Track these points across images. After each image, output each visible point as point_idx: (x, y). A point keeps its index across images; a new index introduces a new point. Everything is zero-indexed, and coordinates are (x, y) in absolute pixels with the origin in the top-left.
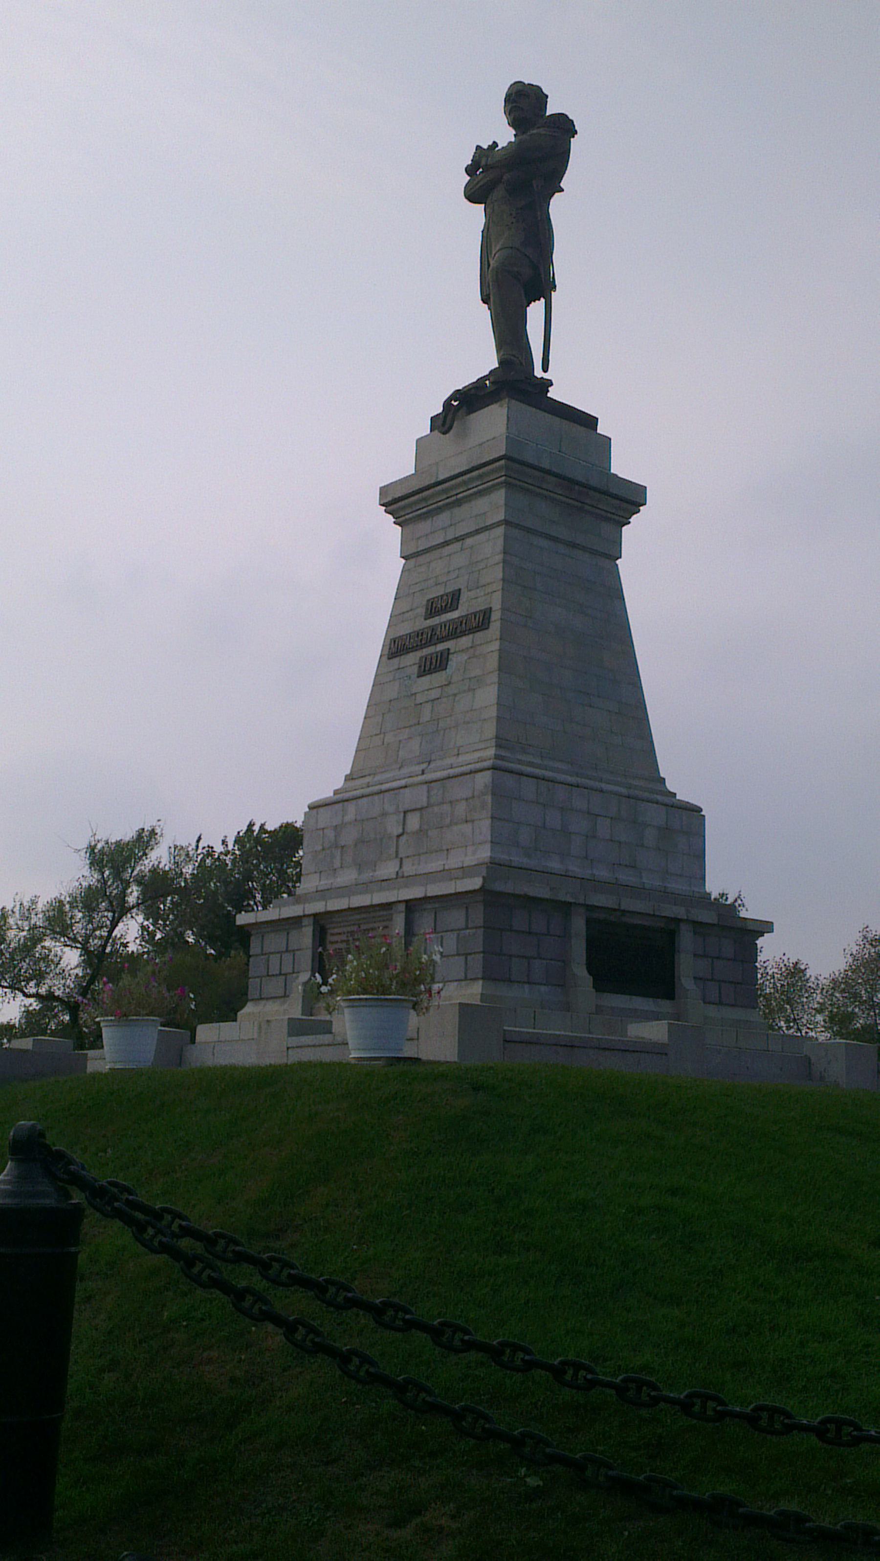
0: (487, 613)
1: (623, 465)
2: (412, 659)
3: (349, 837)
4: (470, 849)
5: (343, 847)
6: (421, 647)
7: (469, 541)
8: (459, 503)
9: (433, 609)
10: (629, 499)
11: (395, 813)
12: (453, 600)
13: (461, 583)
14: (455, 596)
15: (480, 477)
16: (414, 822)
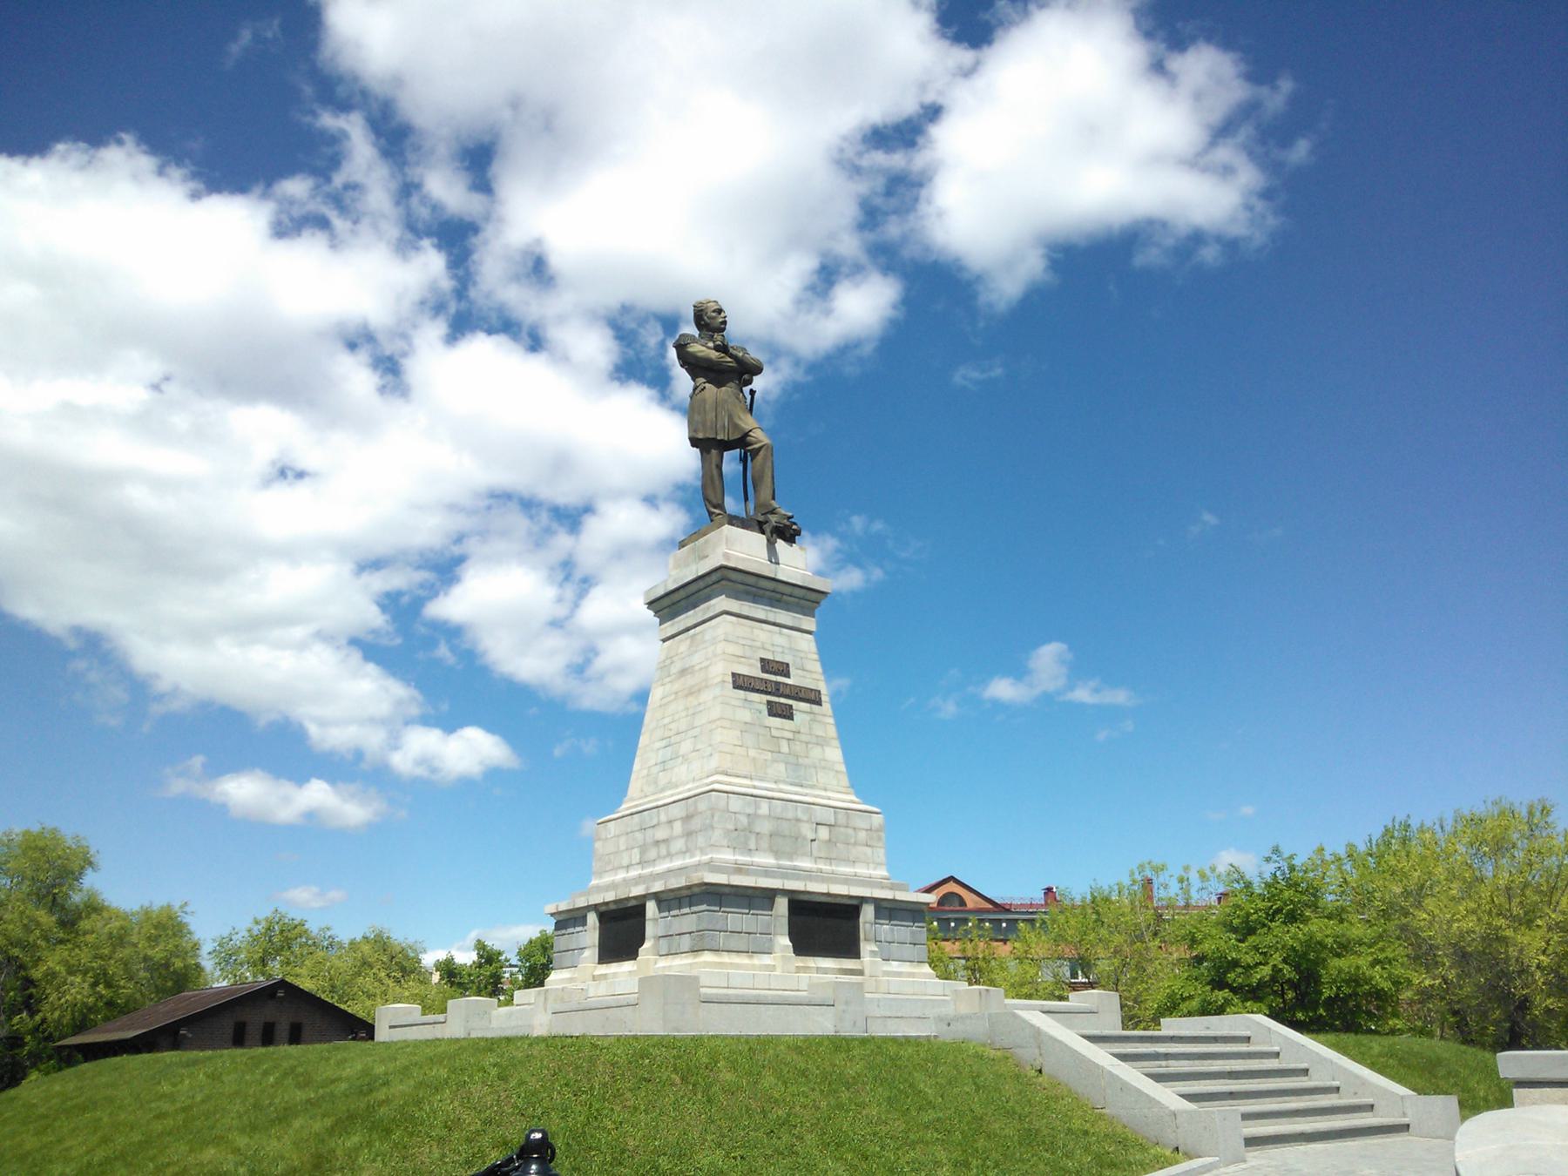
2: (760, 699)
3: (765, 827)
9: (766, 665)
12: (784, 670)
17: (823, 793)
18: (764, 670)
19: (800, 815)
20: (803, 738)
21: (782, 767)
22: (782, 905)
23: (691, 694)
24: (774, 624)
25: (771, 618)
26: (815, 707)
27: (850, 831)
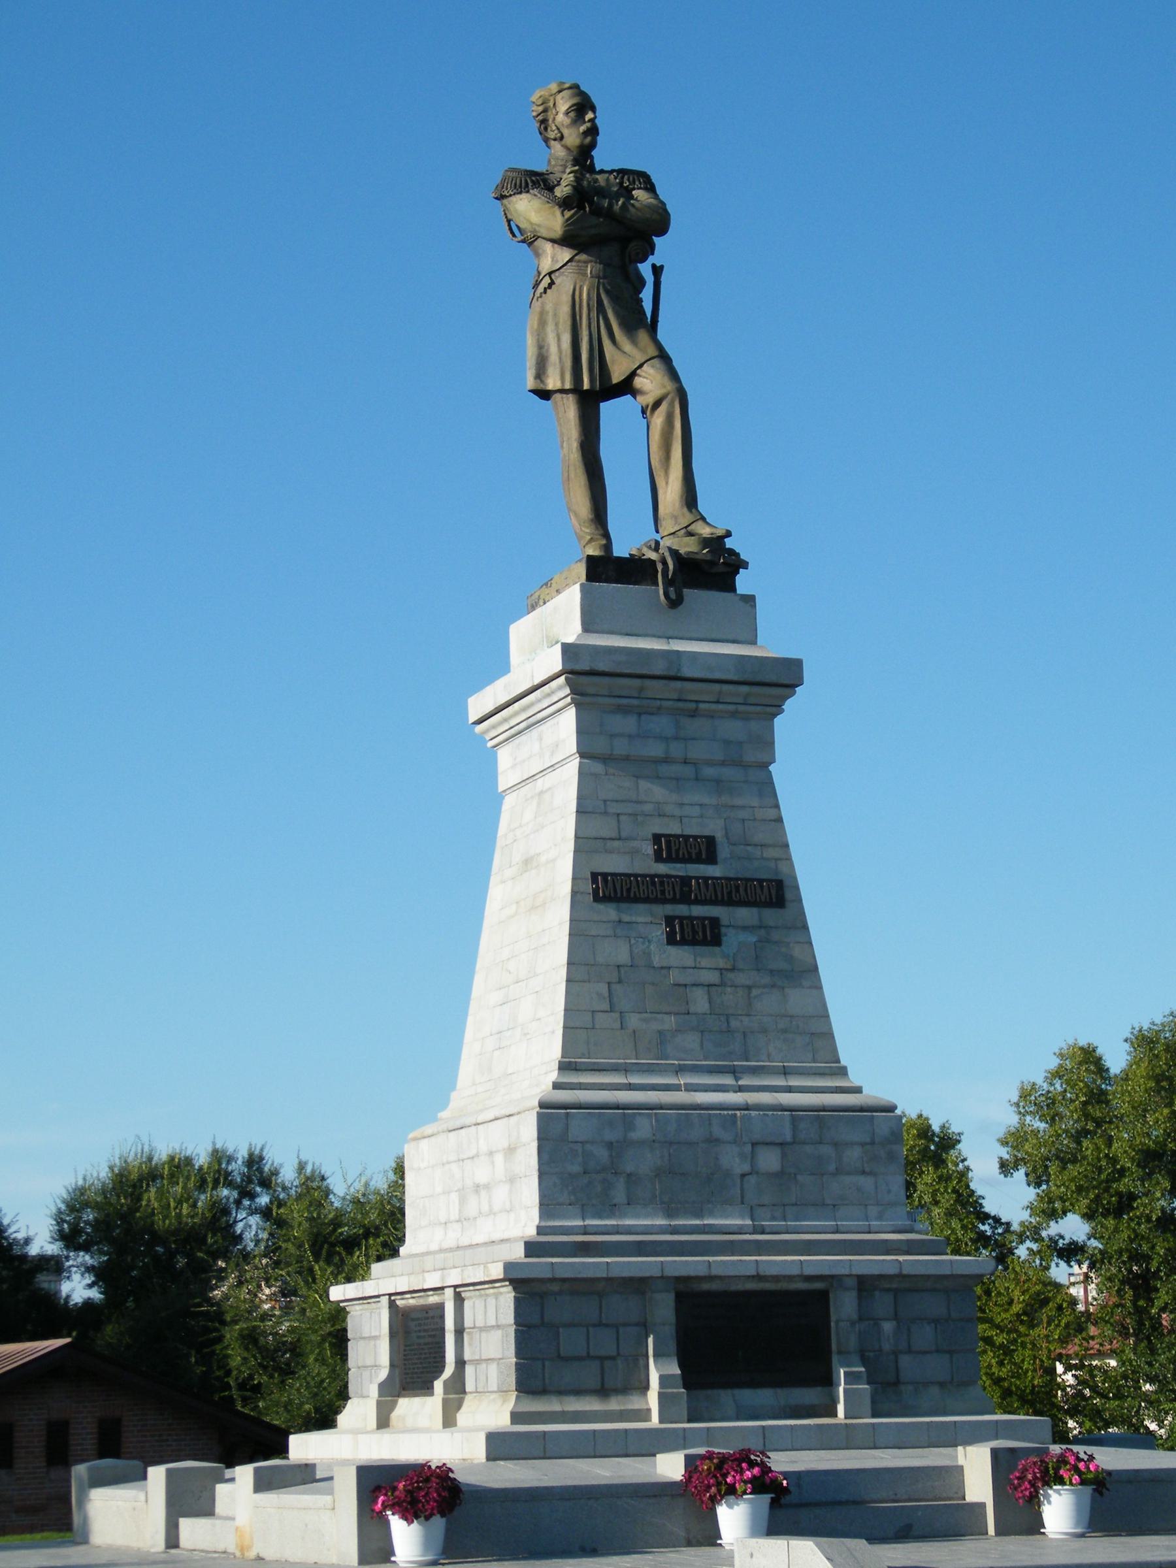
3: (643, 1163)
4: (873, 1210)
5: (629, 1175)
8: (693, 714)
11: (735, 1142)
12: (707, 850)
13: (713, 827)
16: (770, 1160)
17: (780, 1082)
18: (658, 858)
19: (717, 1132)
21: (691, 1040)
22: (664, 1308)
23: (534, 908)
25: (676, 750)
26: (770, 916)
27: (826, 1150)
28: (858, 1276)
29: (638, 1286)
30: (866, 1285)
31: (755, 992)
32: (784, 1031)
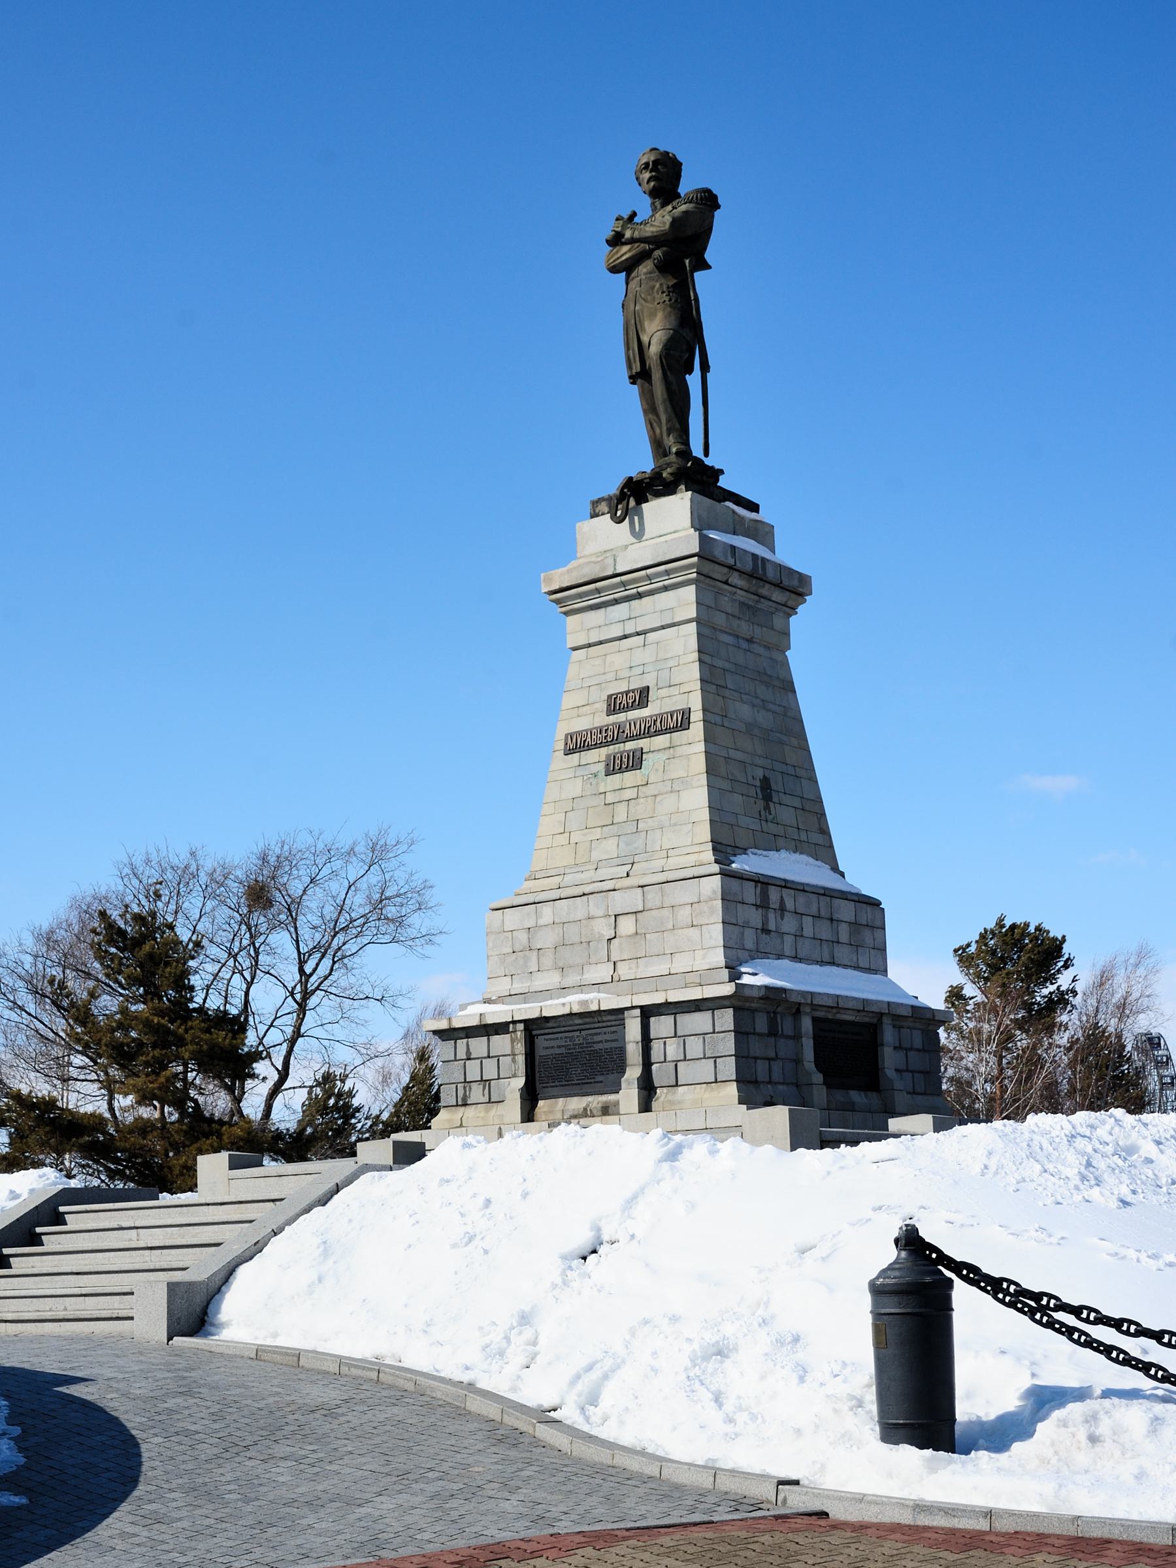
0: (686, 714)
1: (788, 552)
3: (546, 939)
4: (699, 954)
6: (607, 744)
7: (651, 637)
8: (640, 596)
9: (614, 705)
10: (794, 588)
12: (643, 697)
14: (644, 692)
15: (667, 572)
20: (651, 790)
24: (638, 634)
25: (630, 628)
28: (641, 1007)
29: (500, 1028)
30: (647, 1013)
31: (658, 798)
32: (675, 825)
